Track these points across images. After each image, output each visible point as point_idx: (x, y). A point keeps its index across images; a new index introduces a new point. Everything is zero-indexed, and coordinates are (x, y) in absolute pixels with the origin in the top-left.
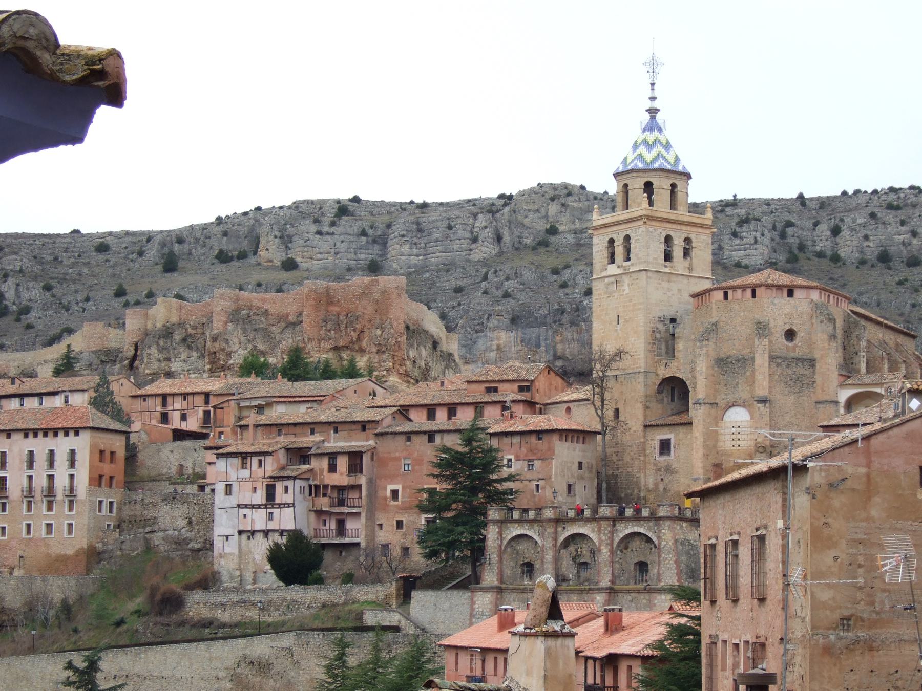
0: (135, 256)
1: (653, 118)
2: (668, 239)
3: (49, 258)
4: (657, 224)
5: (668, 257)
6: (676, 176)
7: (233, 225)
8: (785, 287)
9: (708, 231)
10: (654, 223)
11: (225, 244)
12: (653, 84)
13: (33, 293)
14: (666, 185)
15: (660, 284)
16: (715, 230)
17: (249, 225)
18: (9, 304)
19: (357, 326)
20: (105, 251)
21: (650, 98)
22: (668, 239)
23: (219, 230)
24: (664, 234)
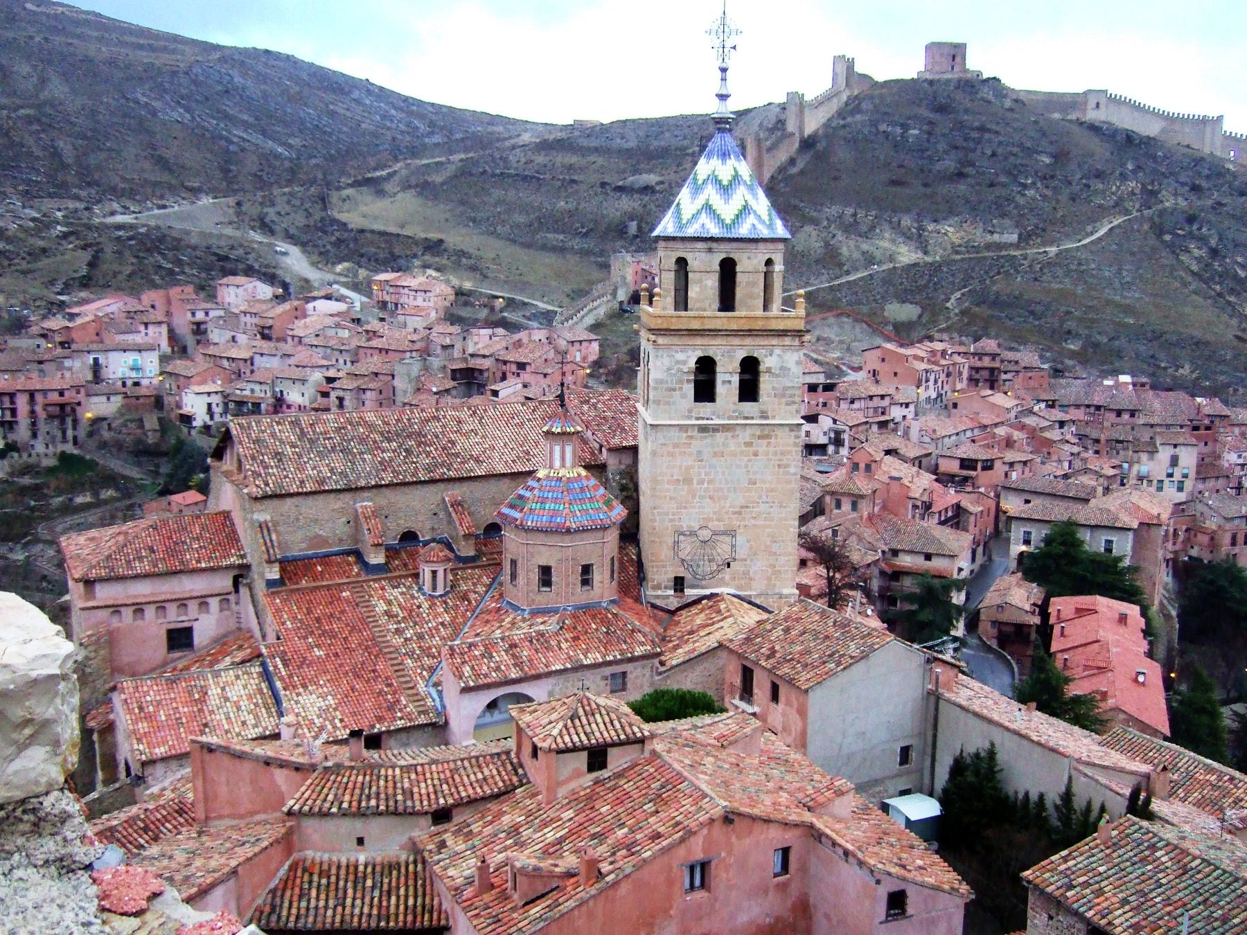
2: (706, 367)
12: (724, 70)
21: (727, 96)
22: (706, 367)
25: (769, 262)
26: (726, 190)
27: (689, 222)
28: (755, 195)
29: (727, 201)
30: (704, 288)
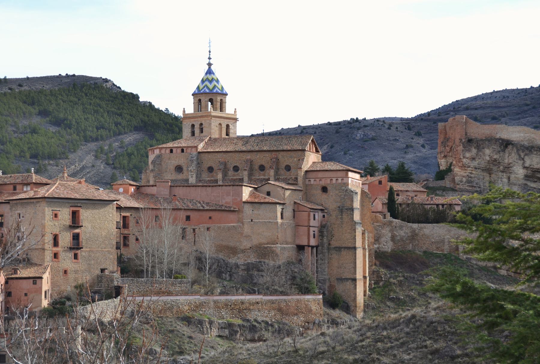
1: (210, 68)
2: (193, 126)
5: (193, 134)
6: (200, 95)
12: (210, 52)
19: (449, 144)
22: (193, 126)
24: (191, 124)
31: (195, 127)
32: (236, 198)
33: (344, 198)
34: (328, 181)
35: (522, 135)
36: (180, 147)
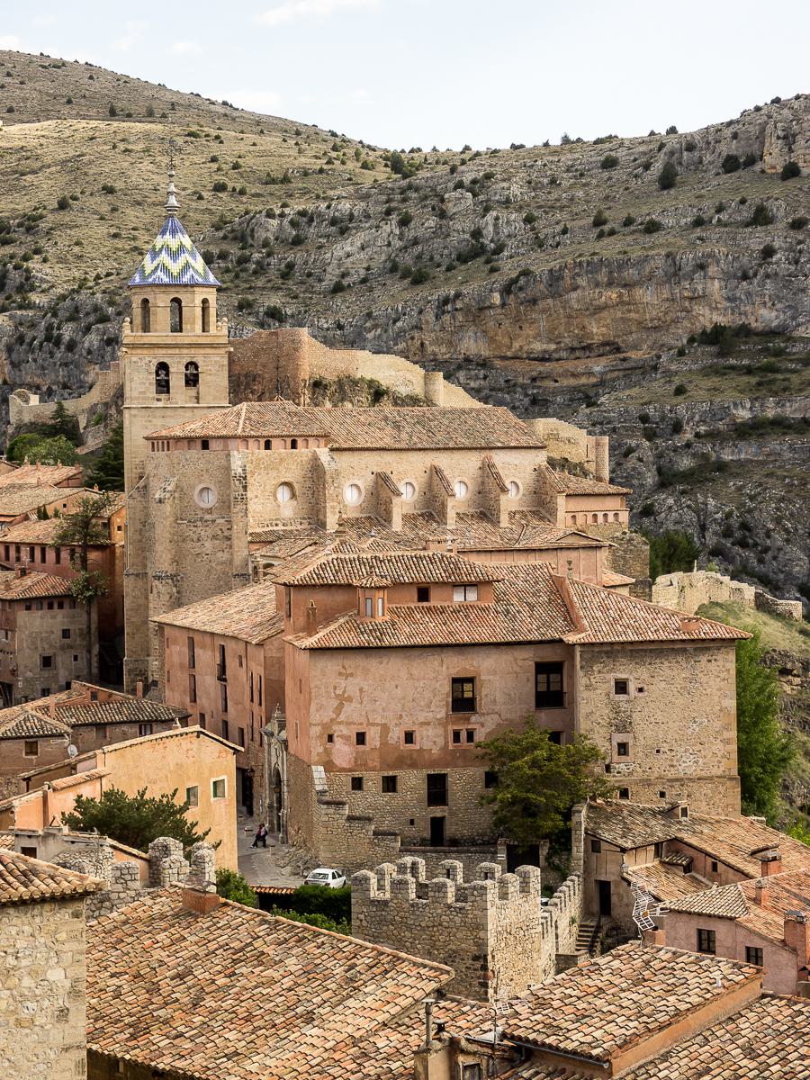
0: (640, 170)
2: (163, 367)
3: (546, 181)
4: (145, 352)
5: (163, 386)
7: (744, 125)
8: (197, 438)
9: (222, 351)
10: (139, 351)
11: (732, 148)
13: (513, 228)
14: (163, 301)
15: (150, 421)
16: (232, 349)
17: (760, 124)
18: (486, 242)
19: (256, 388)
20: (611, 167)
22: (163, 367)
23: (728, 132)
24: (155, 362)
25: (205, 301)
26: (174, 255)
27: (150, 275)
28: (194, 258)
29: (175, 261)
30: (162, 317)
31: (171, 370)
32: (590, 577)
33: (624, 558)
34: (590, 520)
35: (393, 373)
36: (264, 437)
